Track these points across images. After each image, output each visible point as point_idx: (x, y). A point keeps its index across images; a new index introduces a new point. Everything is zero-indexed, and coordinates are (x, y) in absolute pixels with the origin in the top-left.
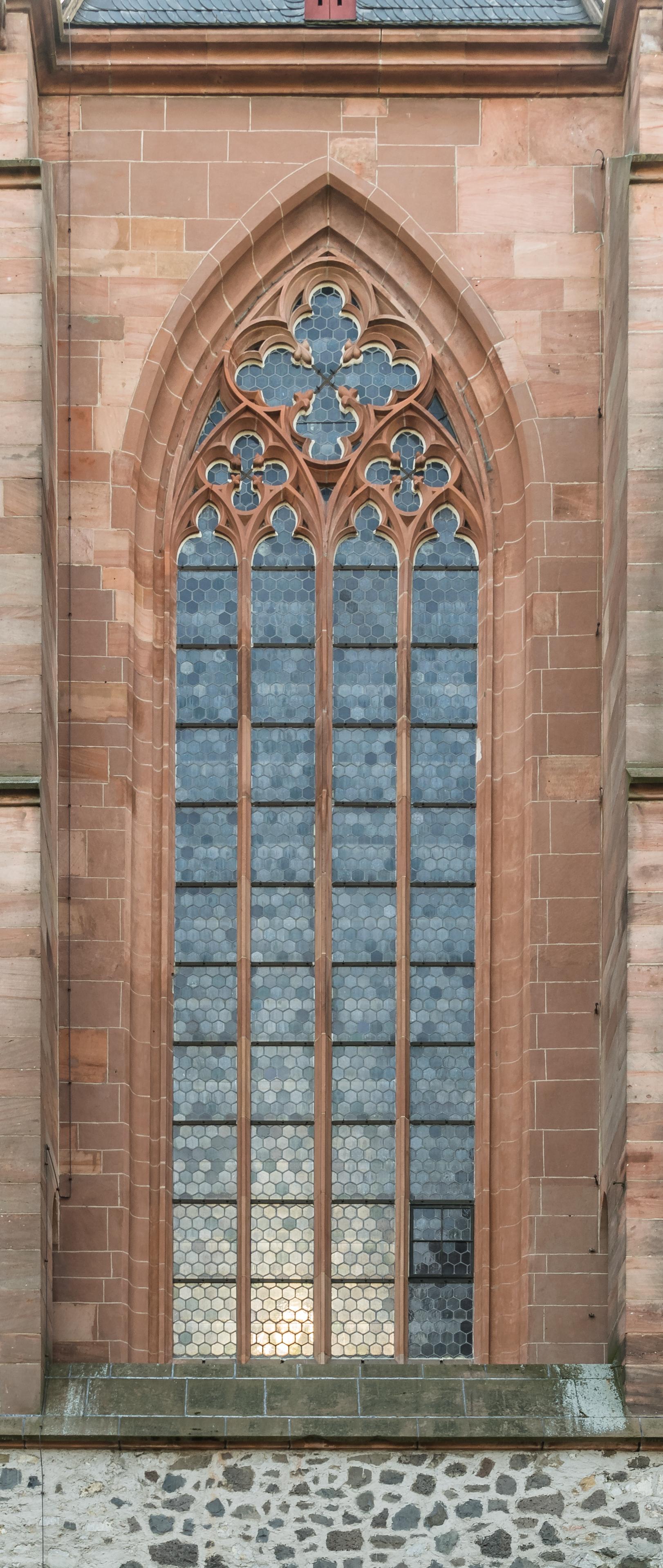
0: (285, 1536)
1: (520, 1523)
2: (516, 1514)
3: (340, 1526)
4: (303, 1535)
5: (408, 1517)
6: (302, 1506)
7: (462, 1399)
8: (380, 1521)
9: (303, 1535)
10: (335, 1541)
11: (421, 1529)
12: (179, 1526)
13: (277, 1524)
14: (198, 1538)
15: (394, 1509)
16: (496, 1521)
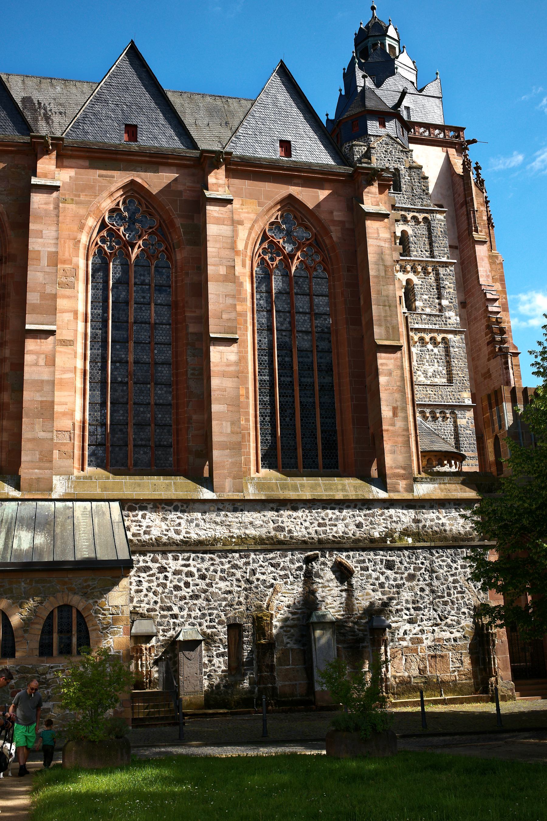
0: (307, 524)
1: (365, 520)
2: (364, 517)
3: (321, 521)
4: (311, 523)
5: (337, 519)
6: (311, 516)
7: (347, 488)
8: (330, 520)
9: (311, 523)
10: (320, 525)
11: (341, 522)
12: (280, 521)
13: (305, 521)
14: (284, 525)
15: (334, 517)
16: (359, 519)
